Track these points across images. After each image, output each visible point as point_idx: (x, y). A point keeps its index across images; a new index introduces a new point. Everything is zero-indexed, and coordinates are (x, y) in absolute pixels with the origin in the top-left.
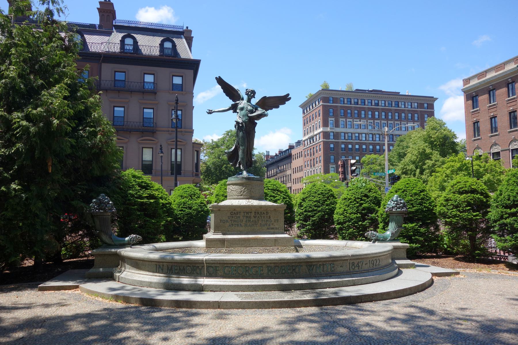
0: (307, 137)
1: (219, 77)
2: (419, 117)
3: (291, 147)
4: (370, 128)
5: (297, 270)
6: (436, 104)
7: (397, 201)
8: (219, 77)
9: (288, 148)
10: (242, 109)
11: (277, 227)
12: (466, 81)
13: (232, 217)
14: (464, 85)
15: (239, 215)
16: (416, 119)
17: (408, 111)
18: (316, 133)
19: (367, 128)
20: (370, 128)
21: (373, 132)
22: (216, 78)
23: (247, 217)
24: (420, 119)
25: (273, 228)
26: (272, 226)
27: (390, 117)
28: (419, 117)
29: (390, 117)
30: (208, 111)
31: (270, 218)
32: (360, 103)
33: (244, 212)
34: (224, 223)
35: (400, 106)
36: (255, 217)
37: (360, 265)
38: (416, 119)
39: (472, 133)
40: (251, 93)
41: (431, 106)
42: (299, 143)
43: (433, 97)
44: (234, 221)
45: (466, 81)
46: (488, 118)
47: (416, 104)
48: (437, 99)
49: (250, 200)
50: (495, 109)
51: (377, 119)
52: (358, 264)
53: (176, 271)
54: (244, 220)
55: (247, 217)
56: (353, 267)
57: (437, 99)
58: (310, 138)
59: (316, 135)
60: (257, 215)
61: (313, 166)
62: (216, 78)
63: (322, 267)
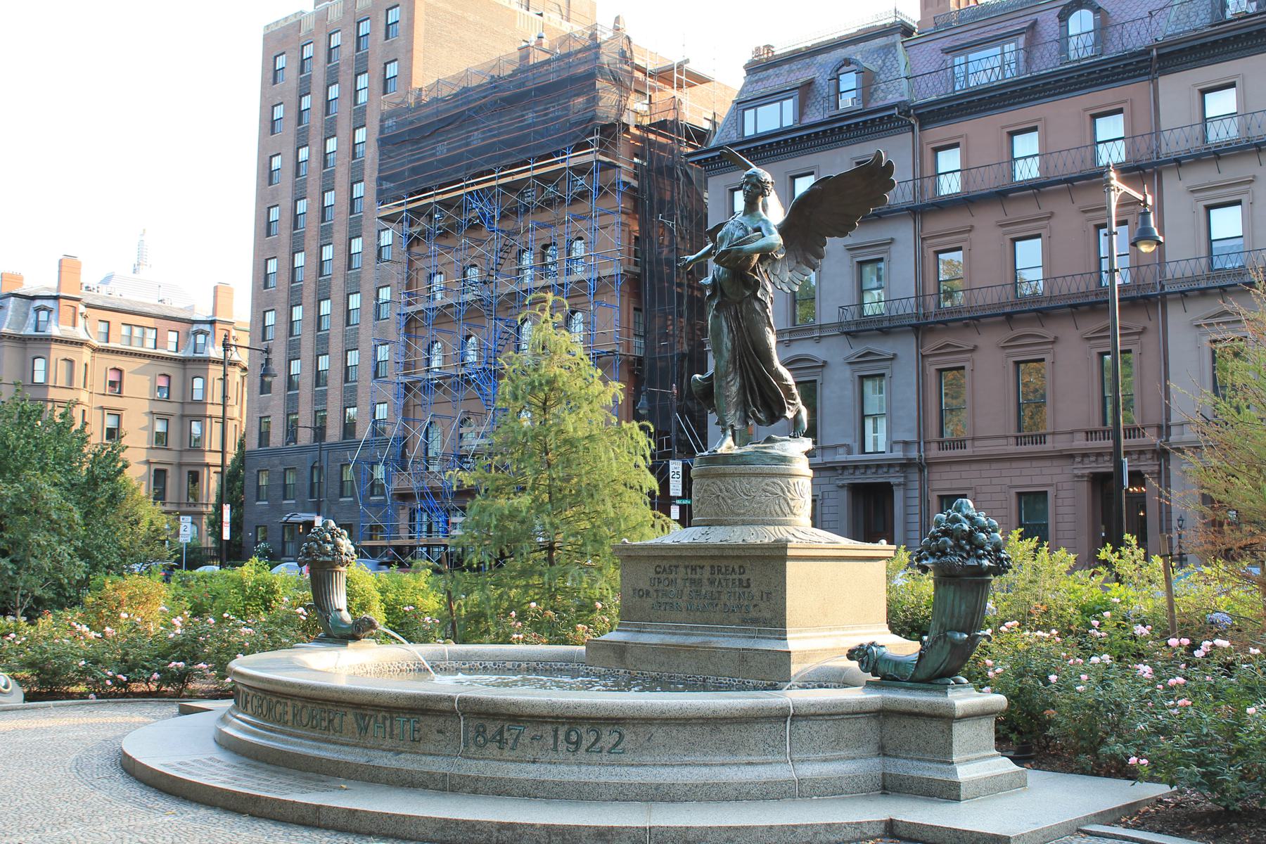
5: (336, 721)
11: (768, 615)
23: (693, 582)
25: (755, 621)
26: (754, 614)
31: (748, 586)
33: (686, 567)
36: (712, 582)
37: (506, 735)
44: (665, 595)
52: (501, 732)
54: (687, 591)
55: (693, 582)
56: (480, 739)
60: (718, 577)
63: (388, 723)
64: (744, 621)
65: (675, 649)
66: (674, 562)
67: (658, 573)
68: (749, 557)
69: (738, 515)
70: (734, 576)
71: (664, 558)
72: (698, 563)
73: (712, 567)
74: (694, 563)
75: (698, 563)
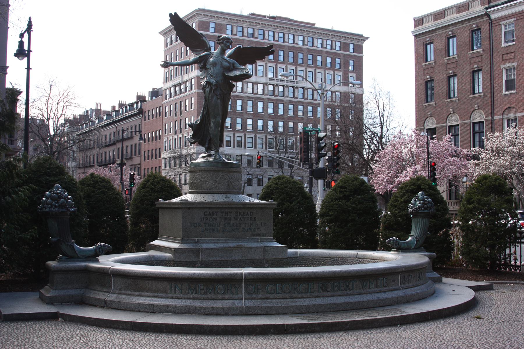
0: (171, 84)
1: (176, 14)
2: (342, 63)
3: (141, 99)
4: (270, 75)
6: (366, 46)
7: (423, 200)
8: (176, 14)
9: (134, 100)
10: (214, 64)
11: (264, 232)
12: (419, 22)
13: (207, 219)
14: (416, 26)
15: (214, 216)
16: (338, 66)
17: (327, 53)
18: (186, 77)
19: (266, 76)
20: (270, 75)
21: (275, 82)
22: (171, 15)
23: (225, 219)
24: (342, 67)
25: (258, 235)
26: (257, 232)
27: (300, 61)
28: (342, 63)
29: (300, 61)
30: (162, 63)
31: (255, 220)
32: (256, 35)
34: (195, 227)
35: (315, 44)
36: (236, 219)
38: (338, 66)
39: (423, 97)
40: (228, 42)
41: (359, 49)
42: (155, 93)
43: (361, 36)
45: (419, 22)
46: (445, 77)
47: (338, 44)
48: (367, 38)
49: (228, 195)
50: (455, 65)
51: (281, 63)
53: (203, 292)
55: (225, 219)
57: (367, 38)
58: (175, 86)
59: (186, 81)
61: (178, 131)
62: (171, 15)
64: (253, 235)
65: (231, 249)
66: (215, 210)
67: (205, 215)
68: (256, 208)
69: (236, 189)
70: (248, 216)
71: (210, 208)
72: (229, 210)
73: (236, 212)
74: (226, 210)
75: (229, 210)
